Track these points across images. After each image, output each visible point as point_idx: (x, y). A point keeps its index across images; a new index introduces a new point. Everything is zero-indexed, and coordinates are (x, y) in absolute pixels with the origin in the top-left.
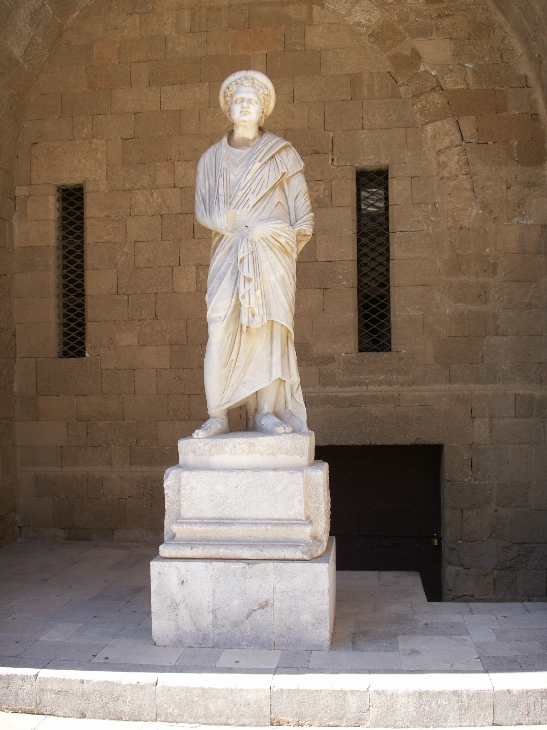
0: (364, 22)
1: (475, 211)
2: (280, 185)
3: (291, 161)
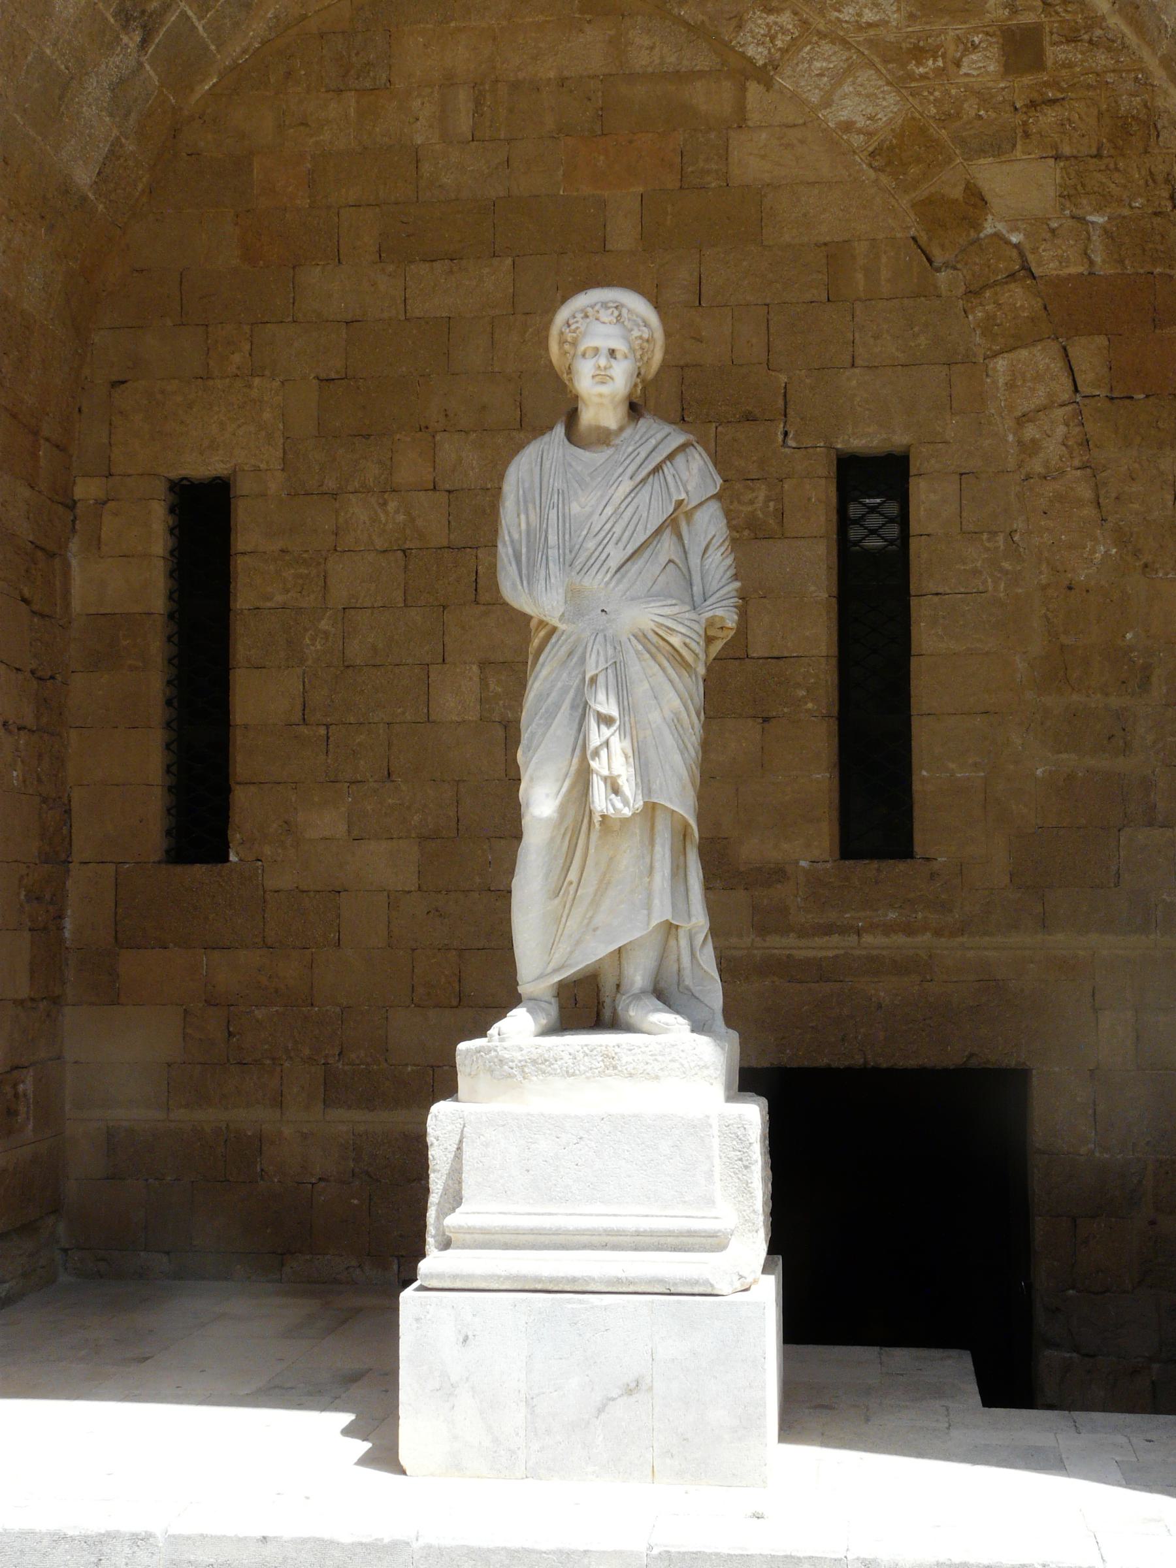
0: (861, 122)
1: (1103, 549)
2: (675, 523)
3: (695, 476)
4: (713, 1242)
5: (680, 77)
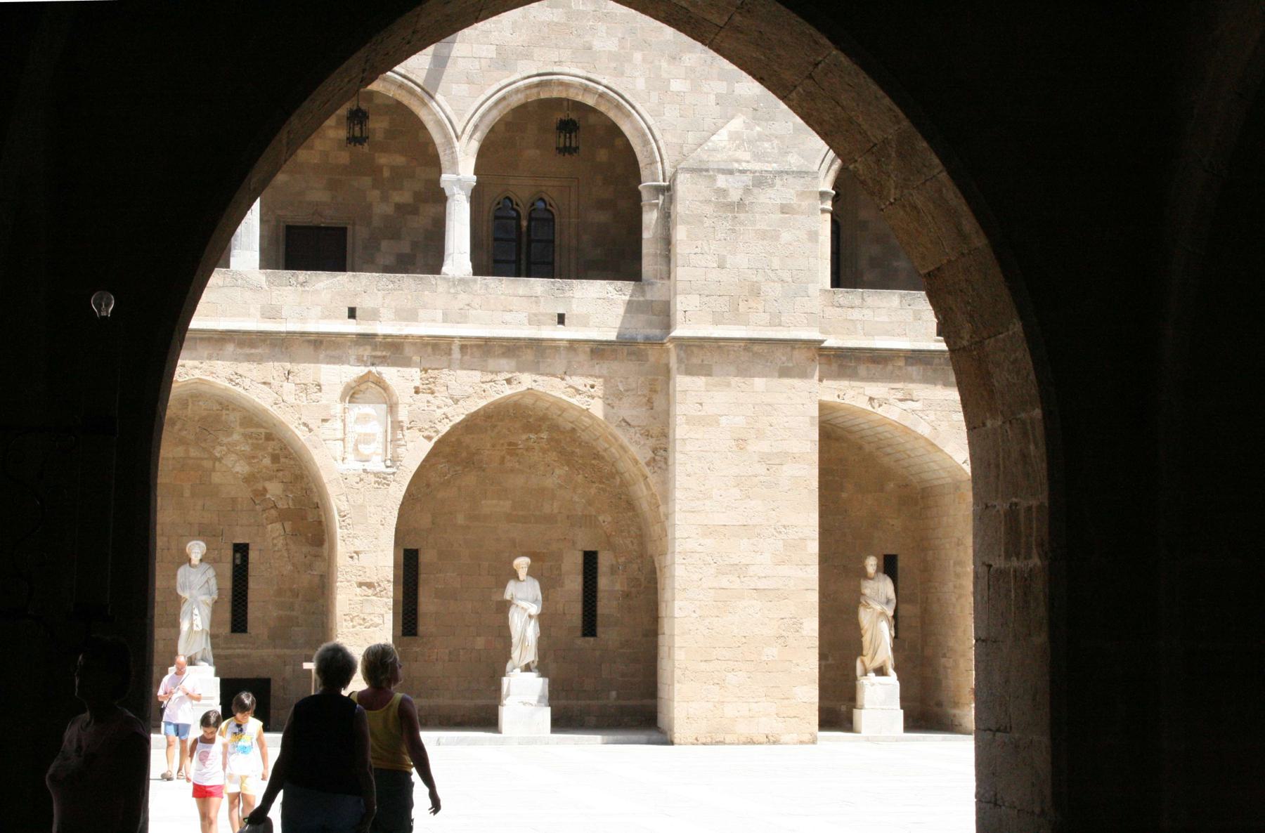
1: (290, 567)
3: (211, 573)
4: (211, 698)
5: (202, 459)
